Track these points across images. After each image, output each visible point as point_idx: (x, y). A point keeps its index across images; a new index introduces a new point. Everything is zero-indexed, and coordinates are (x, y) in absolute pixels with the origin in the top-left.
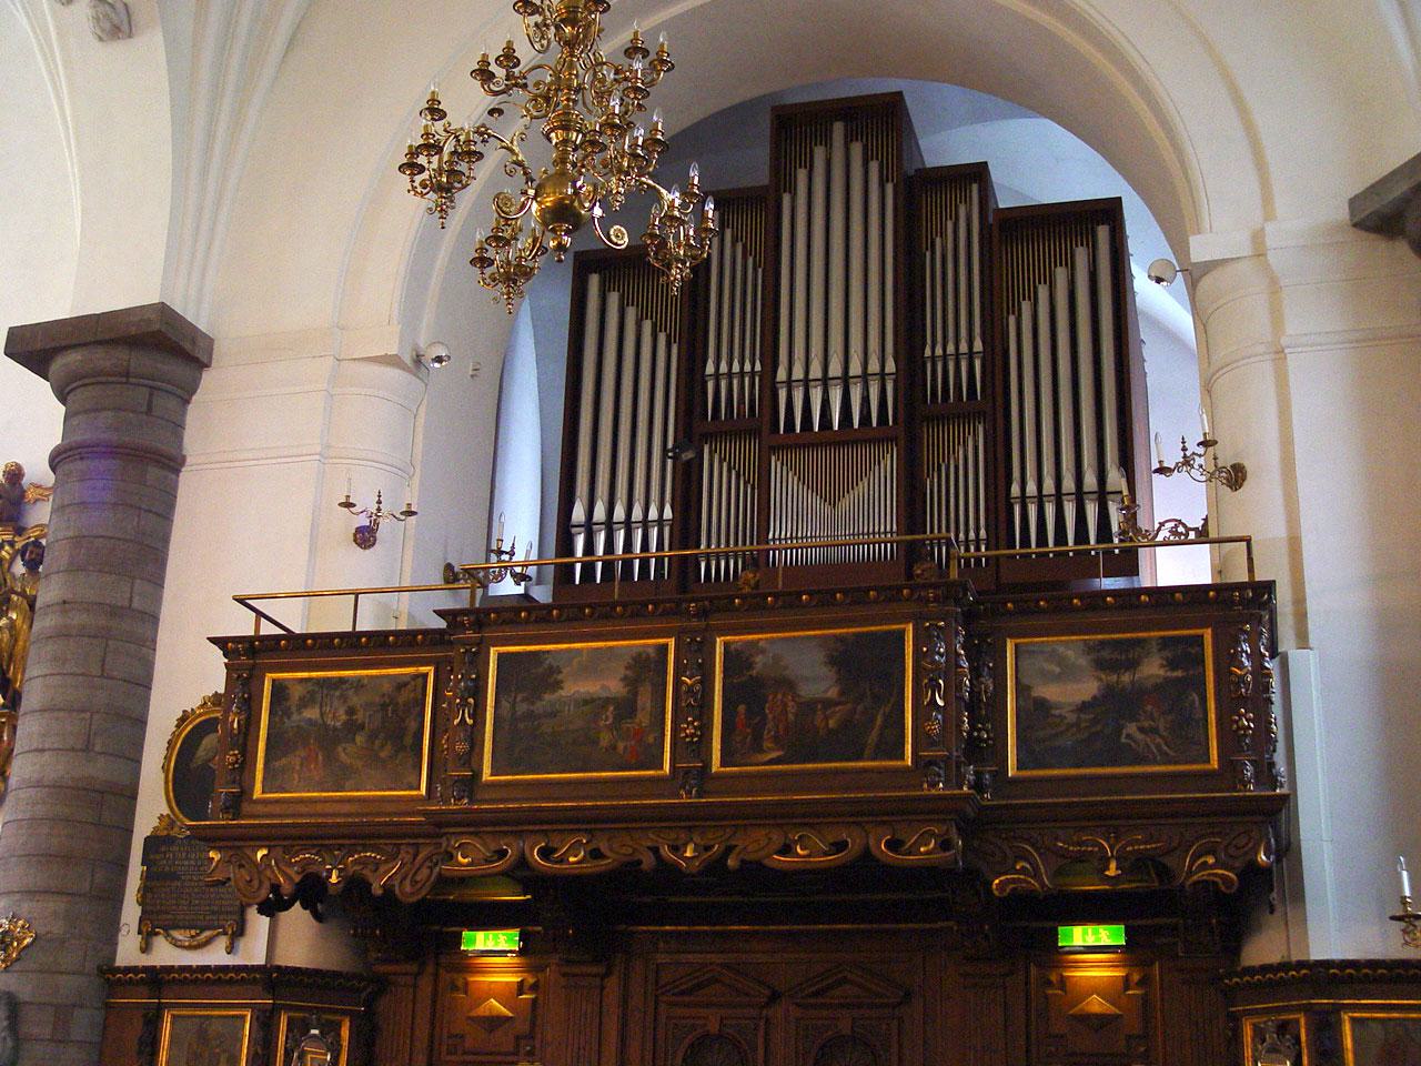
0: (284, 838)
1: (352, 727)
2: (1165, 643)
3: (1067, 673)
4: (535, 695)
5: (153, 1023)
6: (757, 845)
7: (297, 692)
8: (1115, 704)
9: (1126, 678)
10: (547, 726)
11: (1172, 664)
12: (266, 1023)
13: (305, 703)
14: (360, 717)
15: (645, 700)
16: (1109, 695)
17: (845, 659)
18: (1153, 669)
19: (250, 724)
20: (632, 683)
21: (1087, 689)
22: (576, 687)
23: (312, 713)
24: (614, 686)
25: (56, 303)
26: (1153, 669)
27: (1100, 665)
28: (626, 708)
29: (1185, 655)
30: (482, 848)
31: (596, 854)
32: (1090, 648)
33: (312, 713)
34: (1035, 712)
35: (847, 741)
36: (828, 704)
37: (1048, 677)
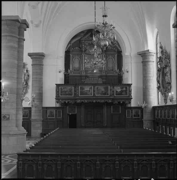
0: (62, 99)
1: (67, 91)
2: (125, 87)
3: (119, 89)
4: (82, 90)
5: (47, 111)
6: (99, 101)
7: (62, 88)
8: (122, 91)
9: (123, 90)
10: (84, 92)
11: (126, 89)
12: (56, 111)
13: (63, 89)
14: (68, 90)
15: (91, 90)
16: (122, 90)
17: (105, 88)
18: (124, 89)
19: (59, 90)
20: (90, 89)
21: (120, 90)
22: (86, 89)
23: (64, 90)
24: (88, 89)
25: (32, 52)
26: (124, 89)
27: (121, 89)
28: (89, 91)
29: (126, 88)
30: (80, 101)
31: (88, 101)
32: (120, 88)
33: (64, 90)
34: (117, 91)
35: (105, 94)
36: (104, 91)
37: (117, 89)
